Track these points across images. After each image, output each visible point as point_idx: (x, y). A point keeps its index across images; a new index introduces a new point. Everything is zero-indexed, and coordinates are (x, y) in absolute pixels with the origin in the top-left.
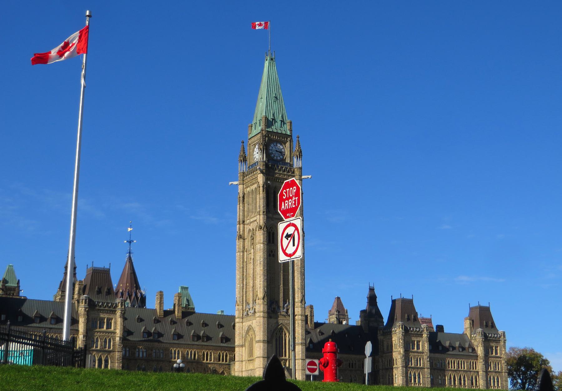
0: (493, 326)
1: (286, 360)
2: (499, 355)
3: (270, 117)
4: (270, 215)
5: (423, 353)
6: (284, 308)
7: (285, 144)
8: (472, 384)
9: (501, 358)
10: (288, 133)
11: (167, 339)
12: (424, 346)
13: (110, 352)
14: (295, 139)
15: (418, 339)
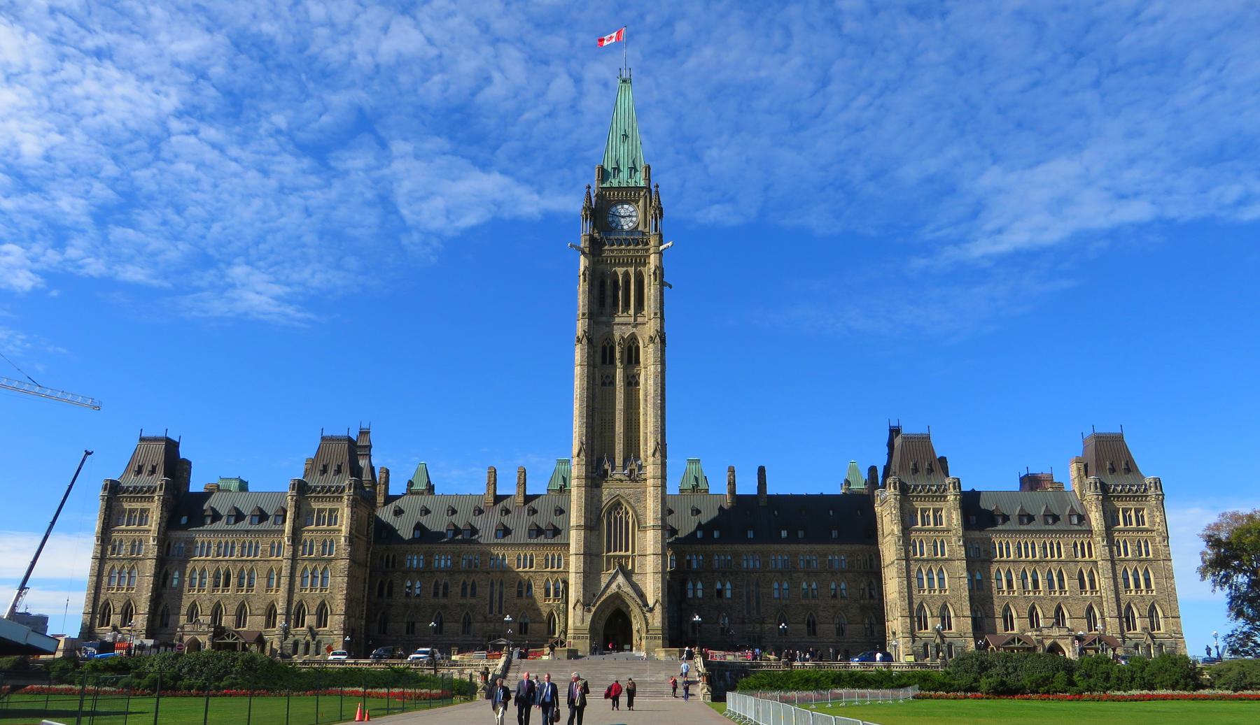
0: (1130, 468)
1: (627, 557)
2: (1147, 526)
3: (609, 167)
4: (604, 318)
5: (949, 531)
6: (624, 468)
7: (637, 202)
8: (1082, 586)
9: (1152, 531)
10: (642, 184)
11: (487, 534)
12: (952, 517)
13: (331, 560)
14: (654, 190)
15: (937, 505)
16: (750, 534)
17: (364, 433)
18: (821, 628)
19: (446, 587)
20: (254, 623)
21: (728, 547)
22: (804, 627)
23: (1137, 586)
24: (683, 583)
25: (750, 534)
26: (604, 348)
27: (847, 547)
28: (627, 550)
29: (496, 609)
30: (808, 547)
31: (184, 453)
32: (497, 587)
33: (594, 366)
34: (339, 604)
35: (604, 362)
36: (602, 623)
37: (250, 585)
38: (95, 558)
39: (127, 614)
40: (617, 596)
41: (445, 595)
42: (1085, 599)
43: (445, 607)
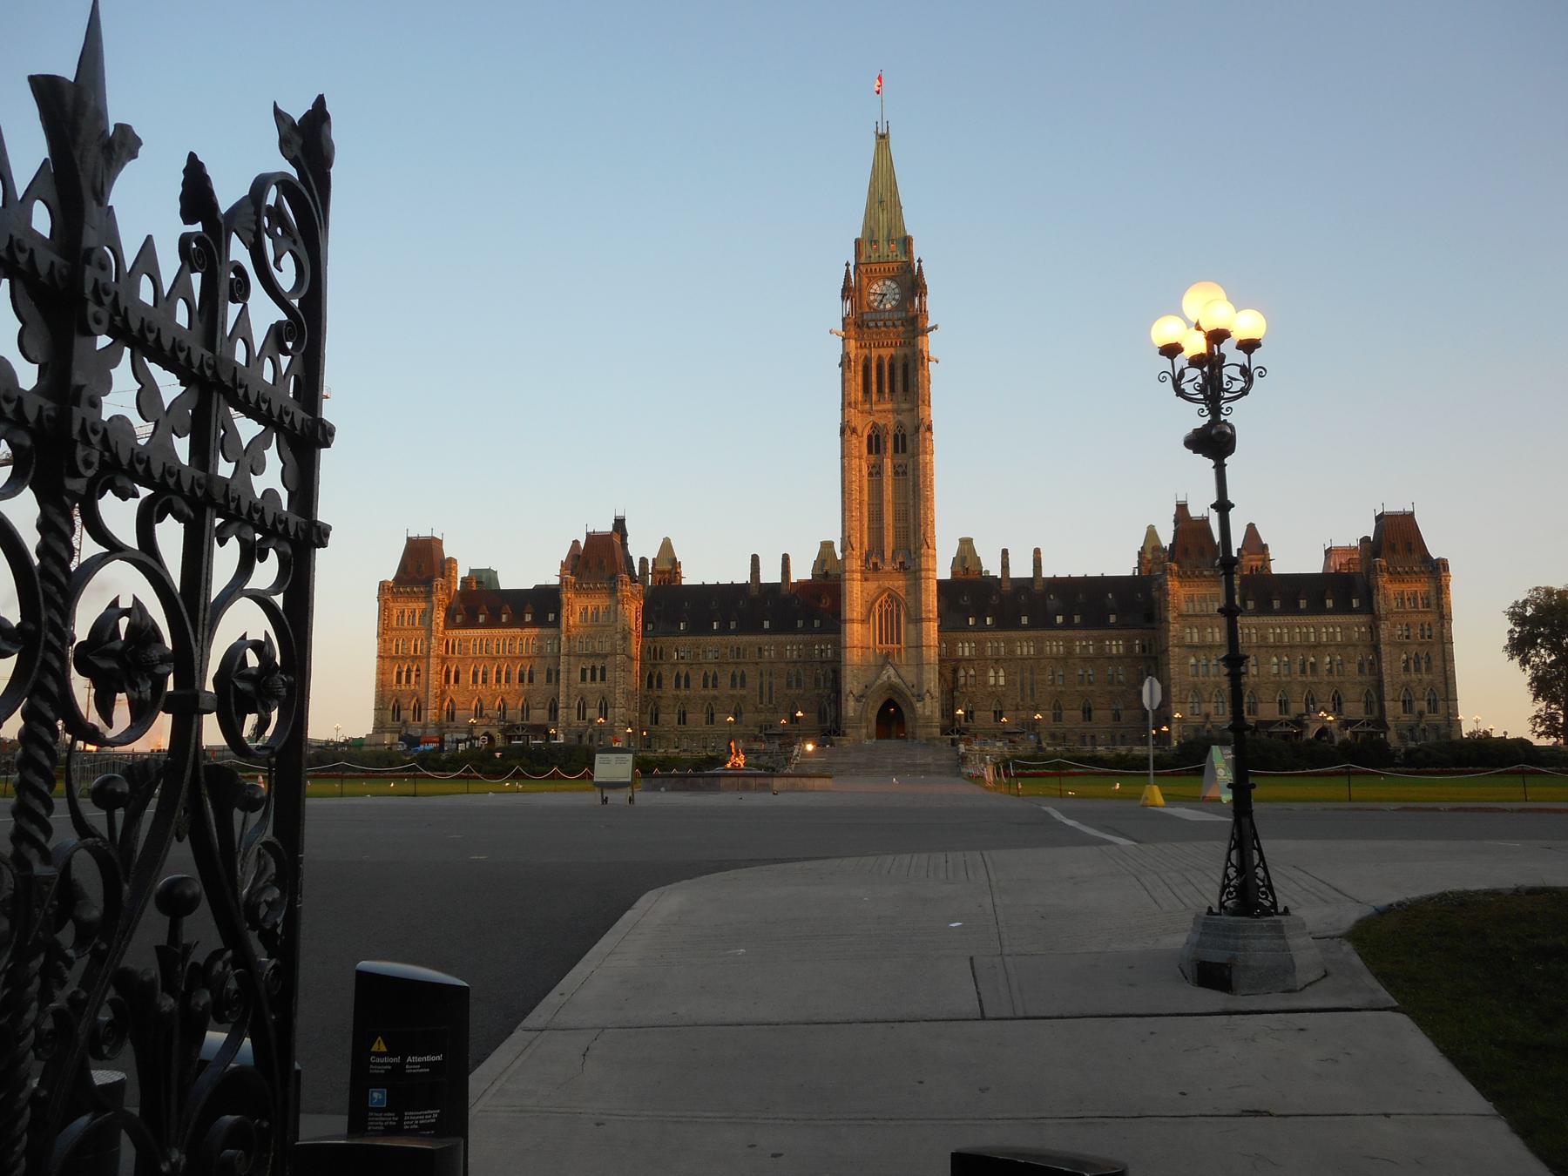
13: (605, 656)
16: (1024, 620)
17: (620, 524)
18: (1096, 714)
19: (715, 678)
20: (539, 716)
21: (1001, 634)
22: (1079, 713)
23: (1418, 670)
24: (955, 671)
25: (1024, 620)
26: (869, 437)
28: (899, 642)
29: (766, 700)
30: (1084, 633)
31: (448, 552)
32: (766, 678)
33: (860, 458)
34: (620, 700)
35: (870, 452)
37: (531, 680)
38: (379, 657)
39: (418, 711)
40: (892, 687)
41: (715, 686)
42: (1361, 683)
43: (715, 698)
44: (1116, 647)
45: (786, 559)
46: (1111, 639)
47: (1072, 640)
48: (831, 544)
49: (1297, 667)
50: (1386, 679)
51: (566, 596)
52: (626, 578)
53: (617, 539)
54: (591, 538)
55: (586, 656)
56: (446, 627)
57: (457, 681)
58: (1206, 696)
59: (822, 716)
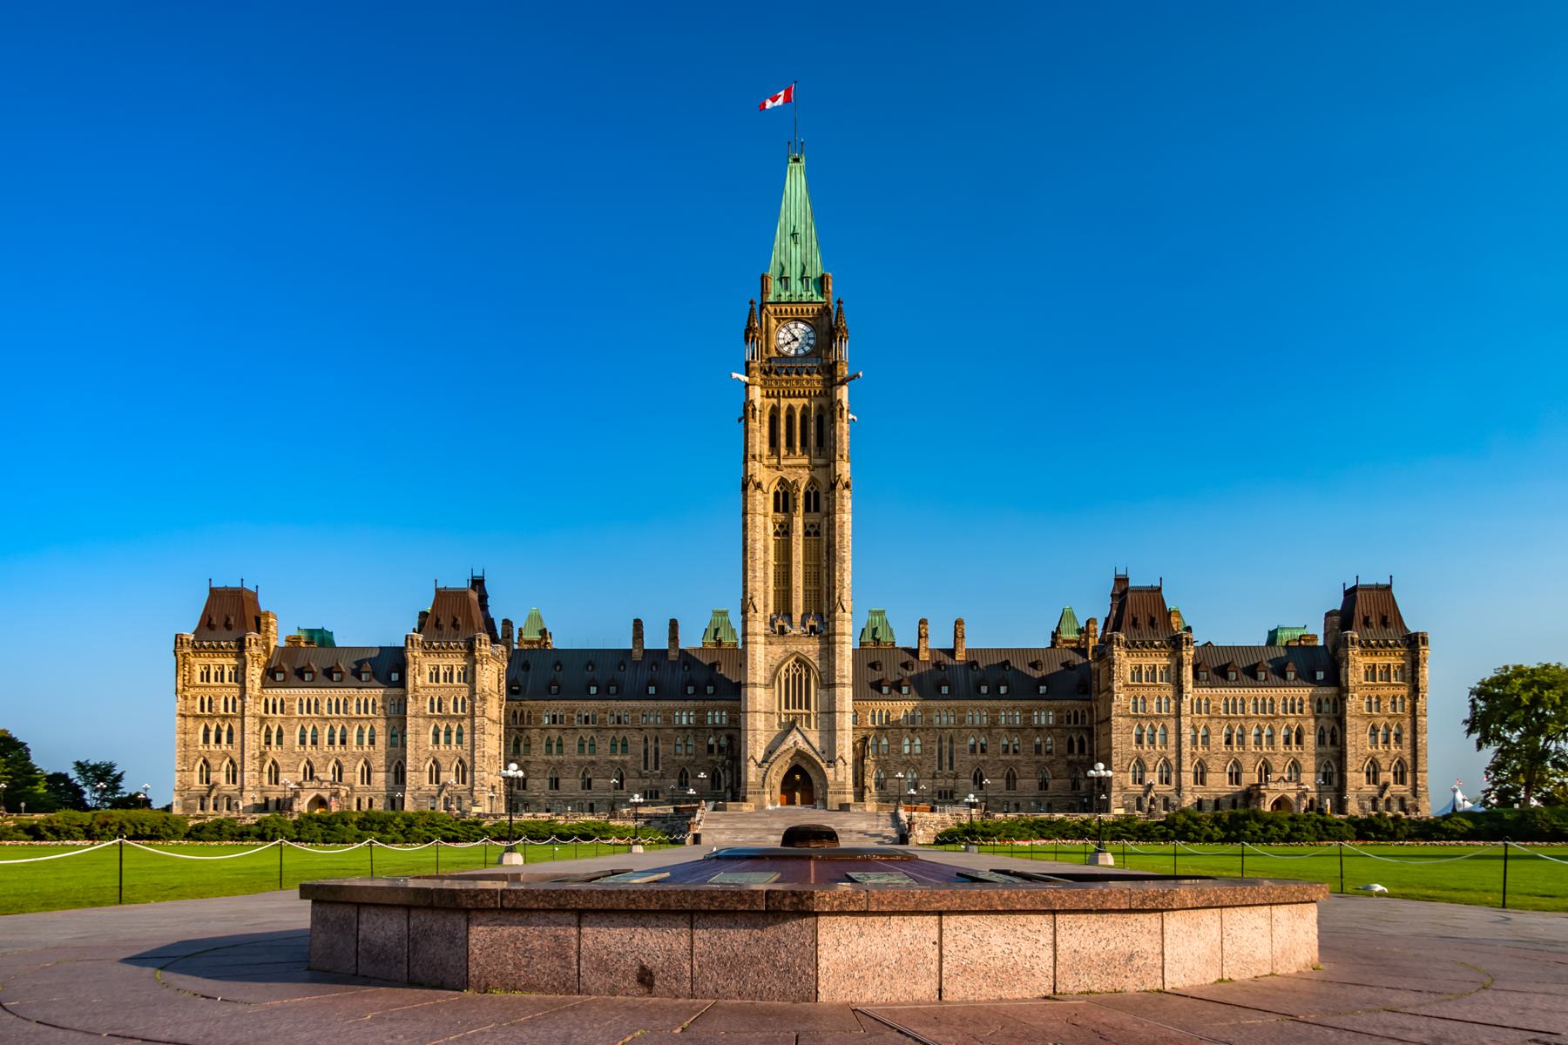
13: (463, 718)
27: (1056, 703)
36: (780, 778)
44: (1044, 718)
45: (674, 625)
46: (1040, 709)
47: (997, 711)
48: (724, 613)
49: (1251, 738)
50: (1350, 750)
51: (414, 654)
52: (485, 637)
53: (474, 596)
54: (442, 595)
55: (438, 717)
56: (263, 686)
57: (280, 742)
58: (1150, 766)
59: (715, 779)
